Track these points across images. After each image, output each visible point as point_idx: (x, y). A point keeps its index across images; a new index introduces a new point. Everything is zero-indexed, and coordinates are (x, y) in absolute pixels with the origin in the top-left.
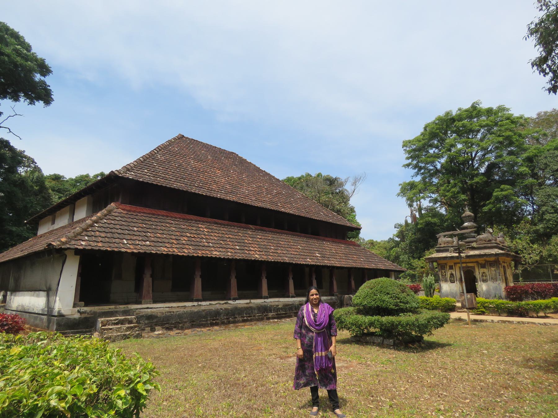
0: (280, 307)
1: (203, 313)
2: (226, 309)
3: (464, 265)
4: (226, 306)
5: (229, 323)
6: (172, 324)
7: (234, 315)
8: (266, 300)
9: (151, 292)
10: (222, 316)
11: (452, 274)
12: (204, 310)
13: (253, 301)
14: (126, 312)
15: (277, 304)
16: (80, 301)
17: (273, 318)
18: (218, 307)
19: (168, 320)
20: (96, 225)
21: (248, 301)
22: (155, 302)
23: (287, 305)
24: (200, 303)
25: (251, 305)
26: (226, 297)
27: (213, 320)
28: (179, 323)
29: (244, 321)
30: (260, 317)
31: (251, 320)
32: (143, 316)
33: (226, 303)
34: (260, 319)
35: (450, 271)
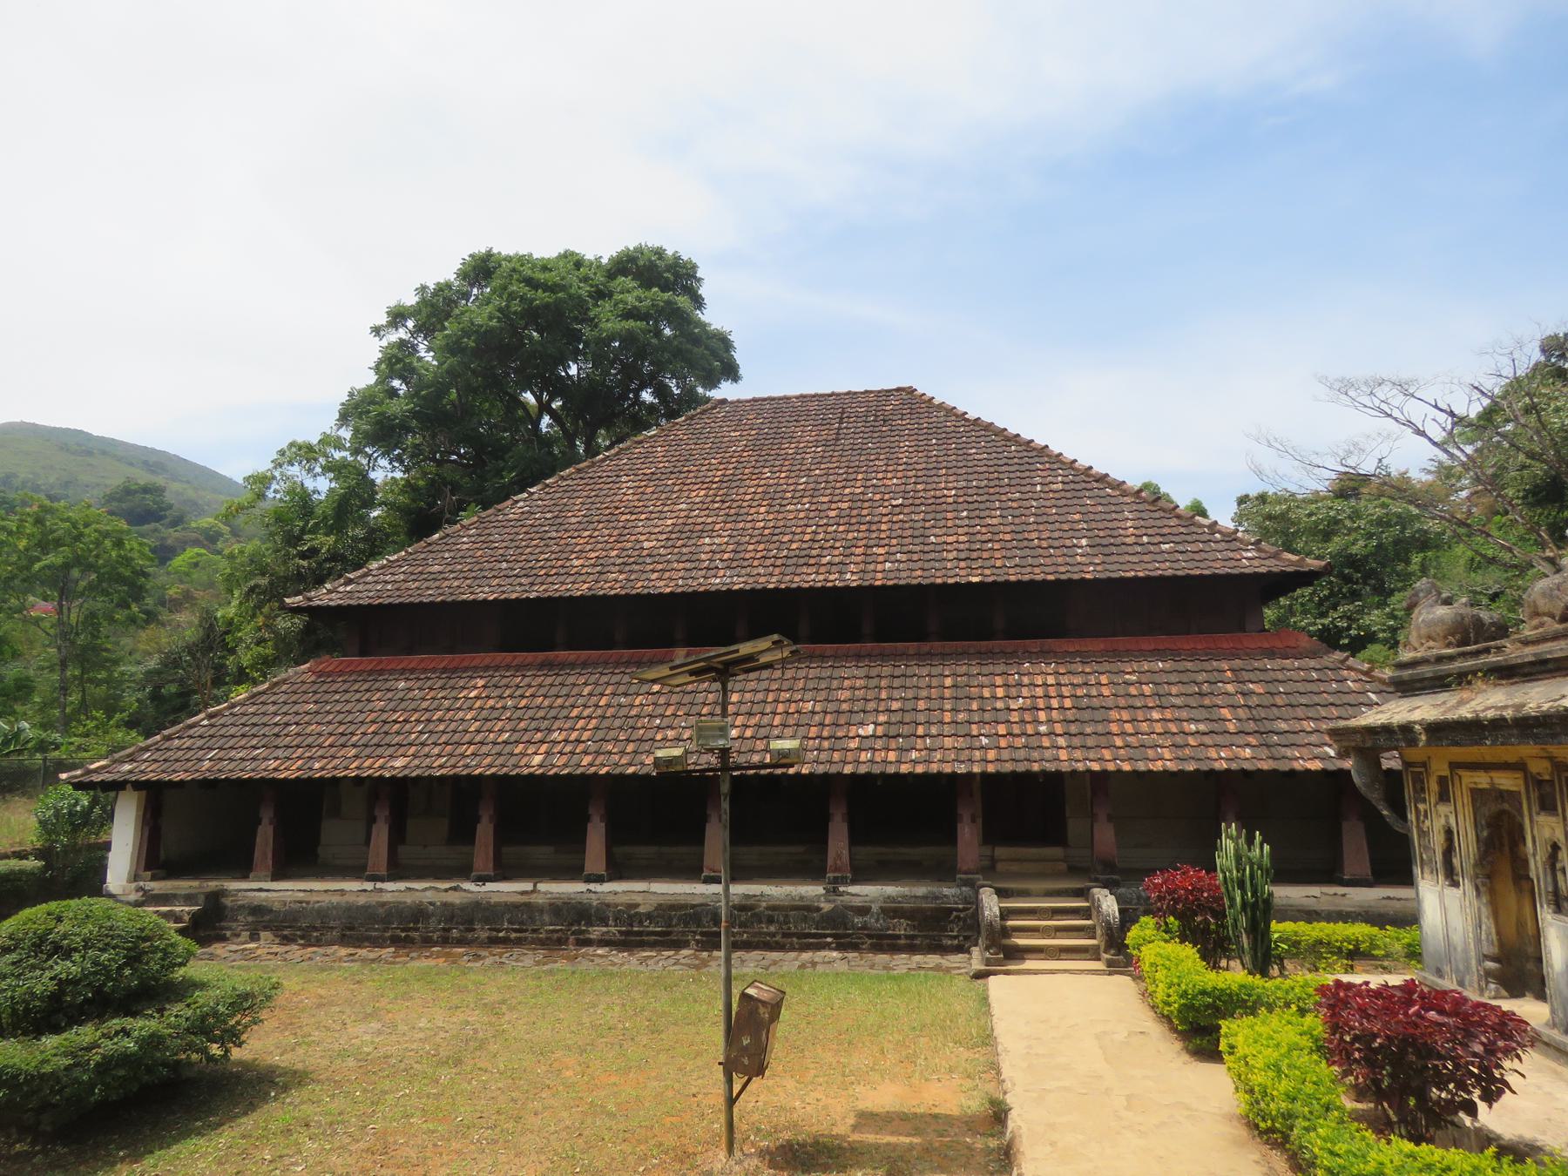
0: (641, 910)
1: (381, 910)
2: (445, 904)
3: (1482, 780)
4: (455, 898)
5: (445, 941)
6: (300, 929)
7: (471, 922)
8: (592, 886)
9: (270, 855)
10: (433, 922)
11: (1449, 833)
12: (383, 904)
13: (542, 887)
14: (189, 899)
15: (638, 899)
16: (147, 868)
17: (603, 943)
18: (429, 896)
19: (295, 920)
20: (205, 722)
21: (528, 886)
22: (276, 877)
23: (672, 907)
24: (379, 885)
25: (534, 899)
26: (463, 871)
27: (403, 930)
28: (316, 929)
29: (493, 942)
30: (556, 936)
31: (519, 942)
32: (242, 906)
33: (455, 889)
34: (553, 944)
35: (1443, 809)
